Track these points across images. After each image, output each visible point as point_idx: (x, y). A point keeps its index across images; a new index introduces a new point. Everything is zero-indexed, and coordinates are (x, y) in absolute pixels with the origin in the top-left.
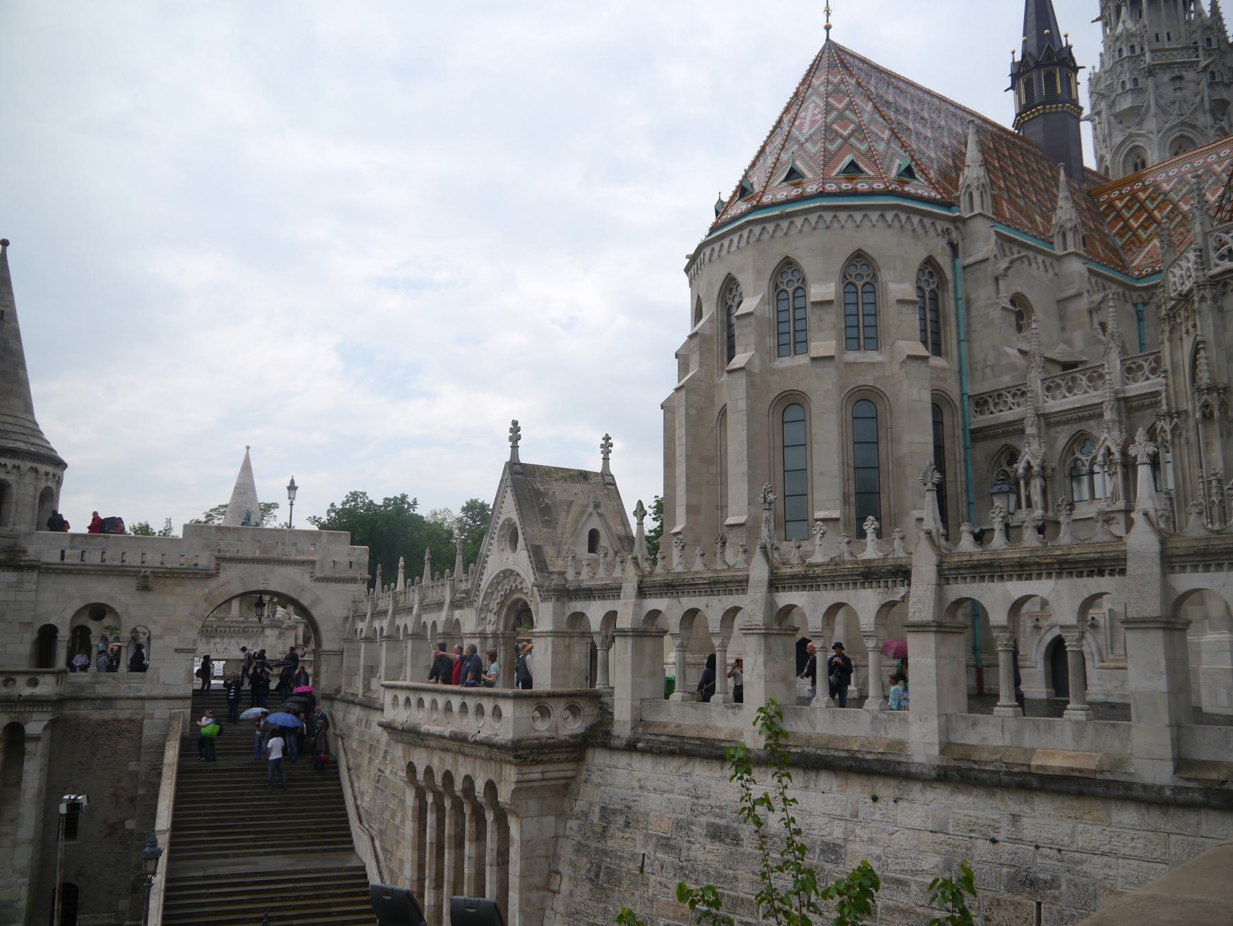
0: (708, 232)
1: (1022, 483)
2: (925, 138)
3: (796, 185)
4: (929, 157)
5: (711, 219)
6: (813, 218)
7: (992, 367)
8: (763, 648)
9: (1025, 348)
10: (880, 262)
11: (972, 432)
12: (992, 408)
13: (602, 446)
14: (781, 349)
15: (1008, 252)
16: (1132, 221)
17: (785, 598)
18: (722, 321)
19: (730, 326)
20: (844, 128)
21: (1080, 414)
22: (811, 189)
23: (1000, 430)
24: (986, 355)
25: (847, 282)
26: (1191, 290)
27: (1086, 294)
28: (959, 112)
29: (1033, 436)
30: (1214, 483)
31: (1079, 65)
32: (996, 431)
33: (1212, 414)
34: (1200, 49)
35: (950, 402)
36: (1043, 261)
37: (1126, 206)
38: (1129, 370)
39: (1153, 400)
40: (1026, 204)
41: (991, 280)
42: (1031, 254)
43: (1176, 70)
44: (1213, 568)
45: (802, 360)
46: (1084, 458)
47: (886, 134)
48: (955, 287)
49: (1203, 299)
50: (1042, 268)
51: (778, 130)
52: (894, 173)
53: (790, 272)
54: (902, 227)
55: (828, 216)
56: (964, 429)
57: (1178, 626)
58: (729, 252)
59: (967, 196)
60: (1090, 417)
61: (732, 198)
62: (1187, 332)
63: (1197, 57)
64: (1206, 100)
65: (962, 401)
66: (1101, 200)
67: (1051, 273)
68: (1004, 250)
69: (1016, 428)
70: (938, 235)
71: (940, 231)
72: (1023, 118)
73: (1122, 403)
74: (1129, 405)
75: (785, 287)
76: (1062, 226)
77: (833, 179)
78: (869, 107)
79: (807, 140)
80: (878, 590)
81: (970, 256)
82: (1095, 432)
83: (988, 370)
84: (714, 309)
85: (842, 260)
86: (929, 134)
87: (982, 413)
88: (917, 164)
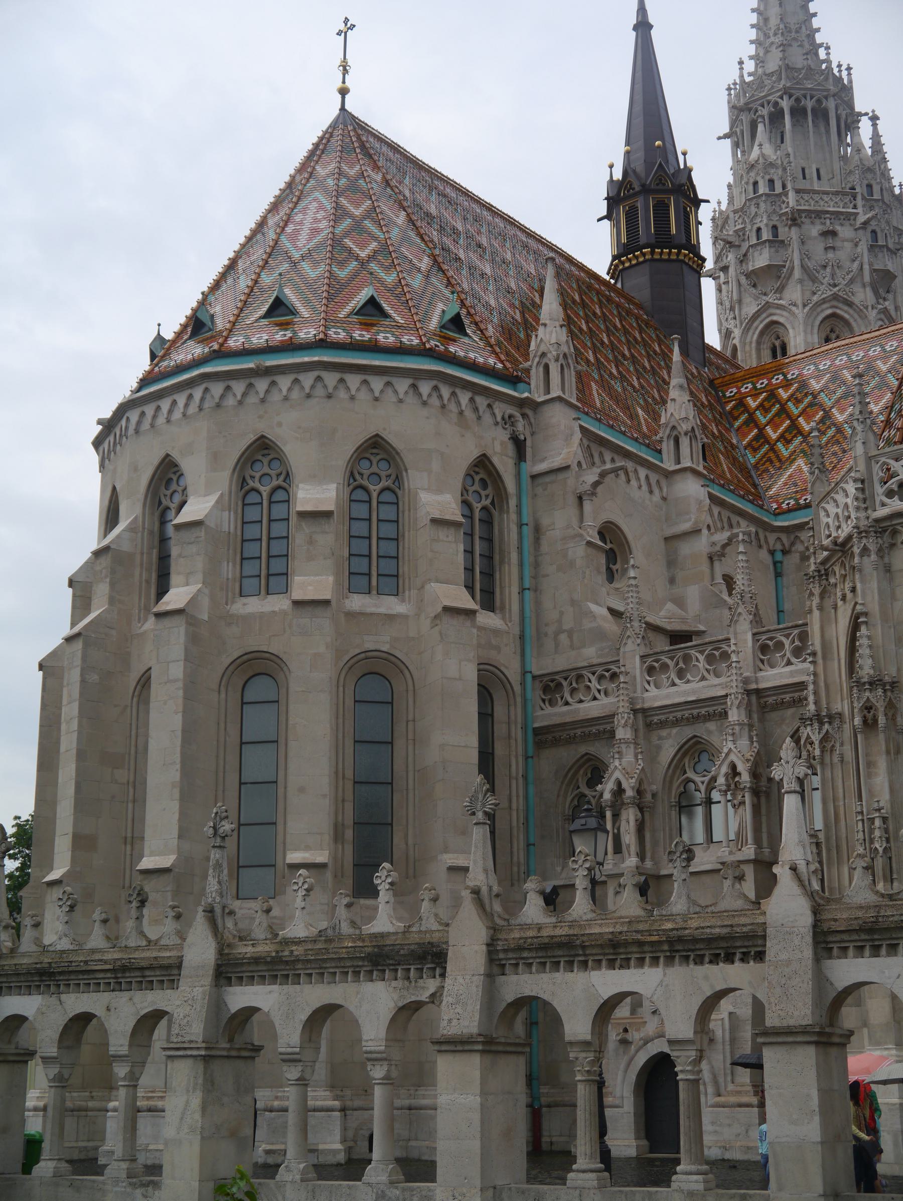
0: (135, 385)
1: (608, 814)
2: (483, 275)
3: (284, 326)
4: (487, 305)
5: (144, 364)
6: (307, 379)
7: (570, 633)
8: (200, 1081)
10: (408, 458)
11: (537, 732)
12: (567, 696)
15: (597, 459)
16: (769, 429)
18: (151, 532)
19: (163, 540)
20: (362, 247)
21: (695, 712)
22: (307, 333)
23: (579, 732)
24: (562, 613)
26: (849, 538)
27: (705, 531)
28: (532, 243)
30: (878, 822)
31: (701, 196)
32: (572, 733)
33: (875, 720)
34: (859, 197)
35: (505, 683)
36: (647, 477)
37: (761, 406)
38: (764, 649)
39: (796, 695)
40: (624, 389)
41: (572, 500)
42: (630, 465)
43: (828, 222)
44: (883, 951)
45: (278, 604)
46: (698, 779)
47: (425, 263)
48: (519, 506)
49: (865, 551)
50: (645, 488)
51: (259, 236)
52: (434, 323)
53: (266, 461)
54: (443, 406)
55: (330, 379)
56: (524, 728)
57: (836, 1040)
58: (168, 421)
59: (541, 369)
60: (708, 717)
61: (179, 335)
62: (844, 598)
63: (855, 207)
64: (866, 267)
65: (523, 683)
67: (656, 497)
68: (592, 456)
70: (497, 424)
71: (499, 419)
72: (623, 263)
73: (754, 698)
74: (762, 701)
75: (257, 485)
76: (674, 428)
78: (401, 219)
80: (394, 983)
81: (543, 460)
82: (715, 740)
83: (563, 637)
84: (138, 510)
85: (349, 449)
86: (488, 270)
87: (552, 703)
88: (469, 313)
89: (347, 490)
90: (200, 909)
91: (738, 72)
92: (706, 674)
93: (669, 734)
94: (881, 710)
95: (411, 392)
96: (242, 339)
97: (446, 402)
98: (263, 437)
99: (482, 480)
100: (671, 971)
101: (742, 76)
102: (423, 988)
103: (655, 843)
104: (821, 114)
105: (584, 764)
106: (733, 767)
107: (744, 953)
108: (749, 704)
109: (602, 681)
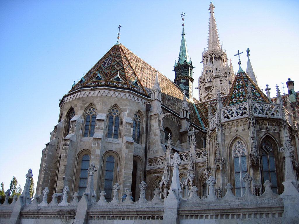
12: (154, 163)
14: (85, 135)
26: (216, 127)
30: (219, 192)
31: (193, 67)
34: (227, 74)
36: (177, 119)
45: (92, 138)
47: (131, 72)
49: (218, 130)
59: (154, 93)
60: (184, 169)
61: (78, 84)
62: (214, 142)
64: (228, 88)
71: (143, 103)
80: (63, 220)
85: (109, 107)
90: (59, 205)
91: (204, 50)
96: (89, 84)
97: (132, 98)
98: (91, 103)
100: (136, 221)
101: (205, 51)
102: (70, 222)
104: (220, 58)
105: (157, 179)
107: (158, 216)
108: (193, 166)
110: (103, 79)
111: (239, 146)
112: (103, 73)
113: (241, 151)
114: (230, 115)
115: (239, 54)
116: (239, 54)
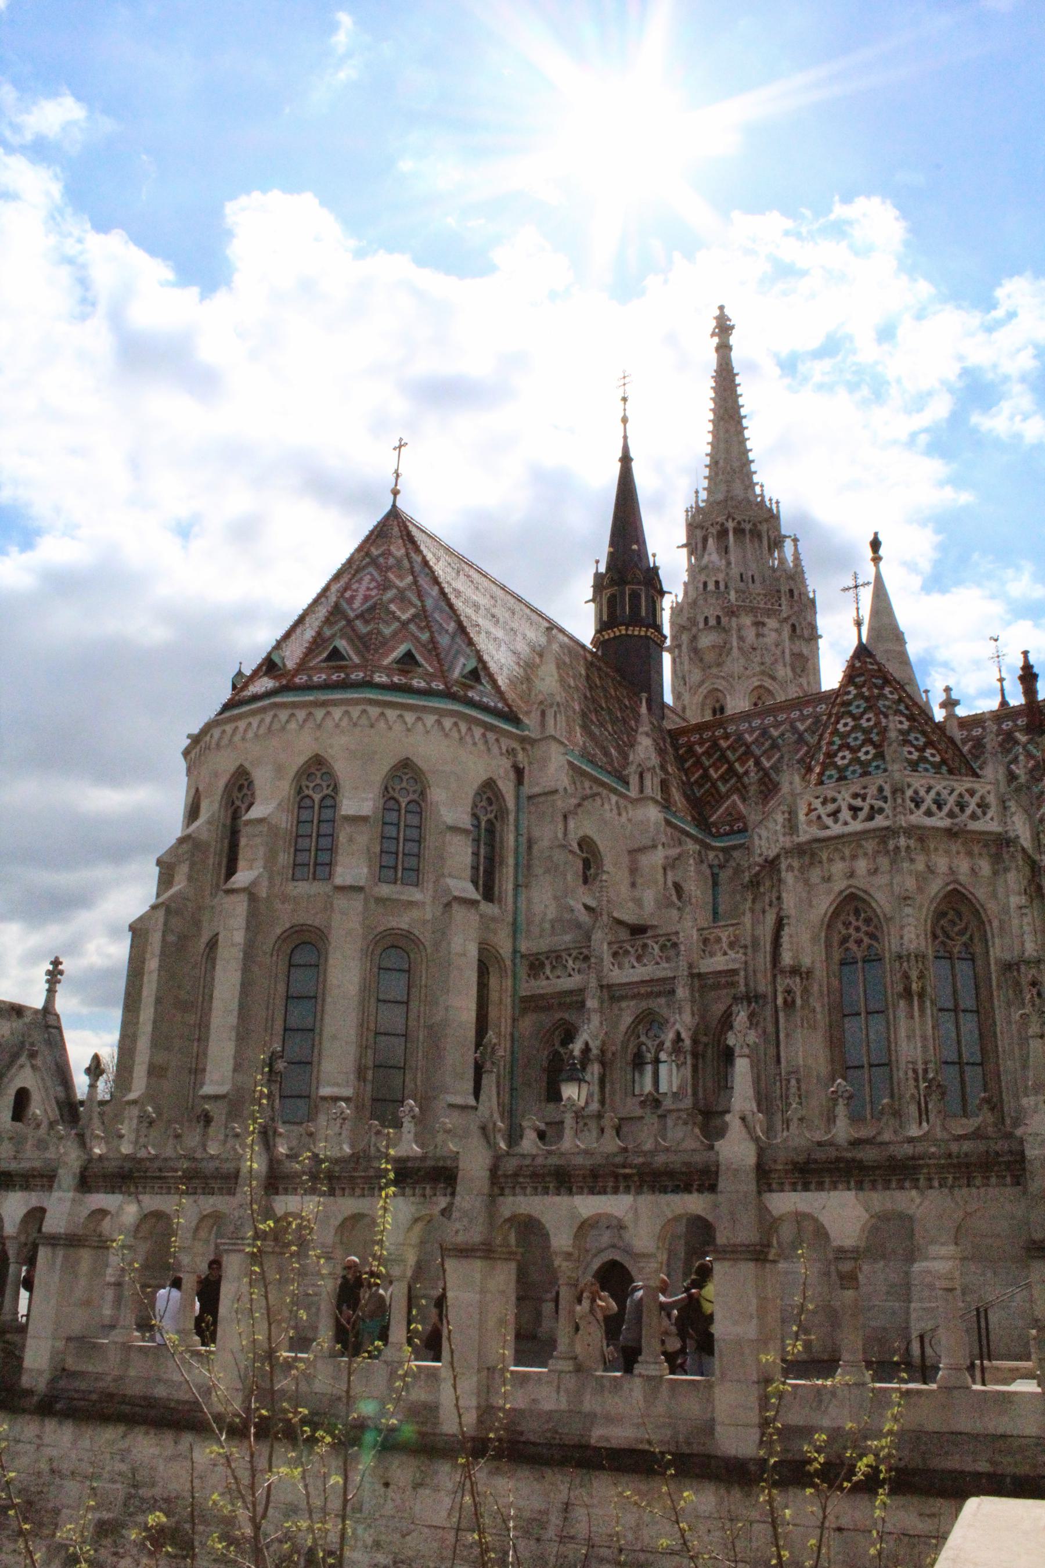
3: (340, 669)
6: (355, 711)
9: (593, 903)
10: (431, 779)
11: (524, 1000)
12: (548, 972)
13: (49, 973)
14: (298, 870)
17: (286, 1204)
20: (404, 611)
22: (357, 675)
25: (389, 798)
26: (778, 856)
29: (595, 1011)
30: (793, 1082)
31: (665, 589)
33: (794, 1002)
34: (783, 599)
35: (499, 960)
36: (617, 803)
38: (705, 941)
41: (560, 818)
42: (605, 792)
44: (813, 1186)
46: (649, 1043)
50: (615, 811)
51: (323, 599)
52: (456, 674)
54: (461, 739)
55: (374, 711)
56: (514, 995)
58: (243, 739)
59: (539, 713)
60: (659, 994)
63: (780, 605)
64: (787, 651)
66: (680, 742)
68: (575, 783)
69: (575, 1001)
70: (502, 754)
71: (504, 751)
75: (311, 793)
77: (386, 668)
79: (357, 617)
80: (412, 1199)
82: (665, 1012)
87: (536, 977)
89: (382, 801)
91: (694, 499)
92: (659, 959)
93: (628, 1006)
94: (798, 993)
95: (436, 727)
96: (305, 678)
99: (489, 799)
101: (697, 502)
103: (613, 1093)
104: (756, 534)
106: (678, 1034)
109: (577, 963)
110: (356, 660)
111: (860, 923)
112: (351, 633)
113: (866, 940)
114: (829, 816)
115: (856, 587)
116: (856, 587)
